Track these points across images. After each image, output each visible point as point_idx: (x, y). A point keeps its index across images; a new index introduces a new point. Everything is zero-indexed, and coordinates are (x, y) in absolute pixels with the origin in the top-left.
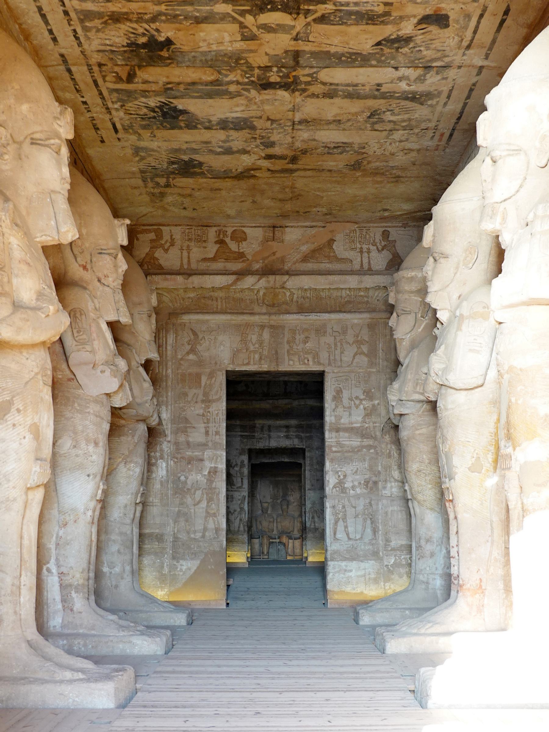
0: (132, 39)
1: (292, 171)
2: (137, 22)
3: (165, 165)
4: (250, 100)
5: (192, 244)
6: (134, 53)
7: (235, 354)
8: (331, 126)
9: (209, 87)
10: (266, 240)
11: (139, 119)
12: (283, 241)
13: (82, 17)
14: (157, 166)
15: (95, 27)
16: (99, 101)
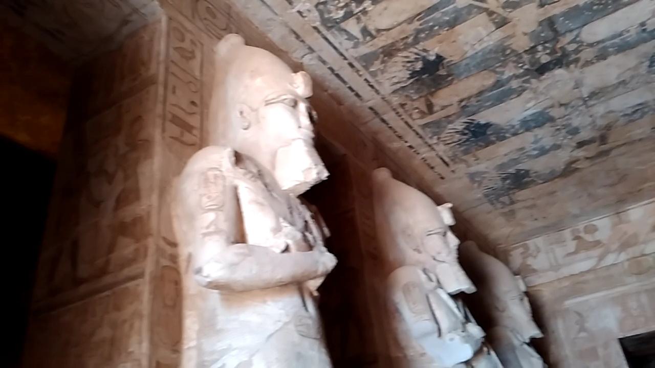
0: (411, 68)
1: (606, 153)
2: (405, 49)
3: (500, 184)
4: (535, 91)
5: (554, 246)
6: (419, 82)
7: (621, 323)
8: (620, 90)
9: (494, 92)
10: (615, 225)
11: (458, 146)
12: (628, 222)
13: (364, 64)
14: (496, 186)
15: (379, 69)
16: (420, 141)
